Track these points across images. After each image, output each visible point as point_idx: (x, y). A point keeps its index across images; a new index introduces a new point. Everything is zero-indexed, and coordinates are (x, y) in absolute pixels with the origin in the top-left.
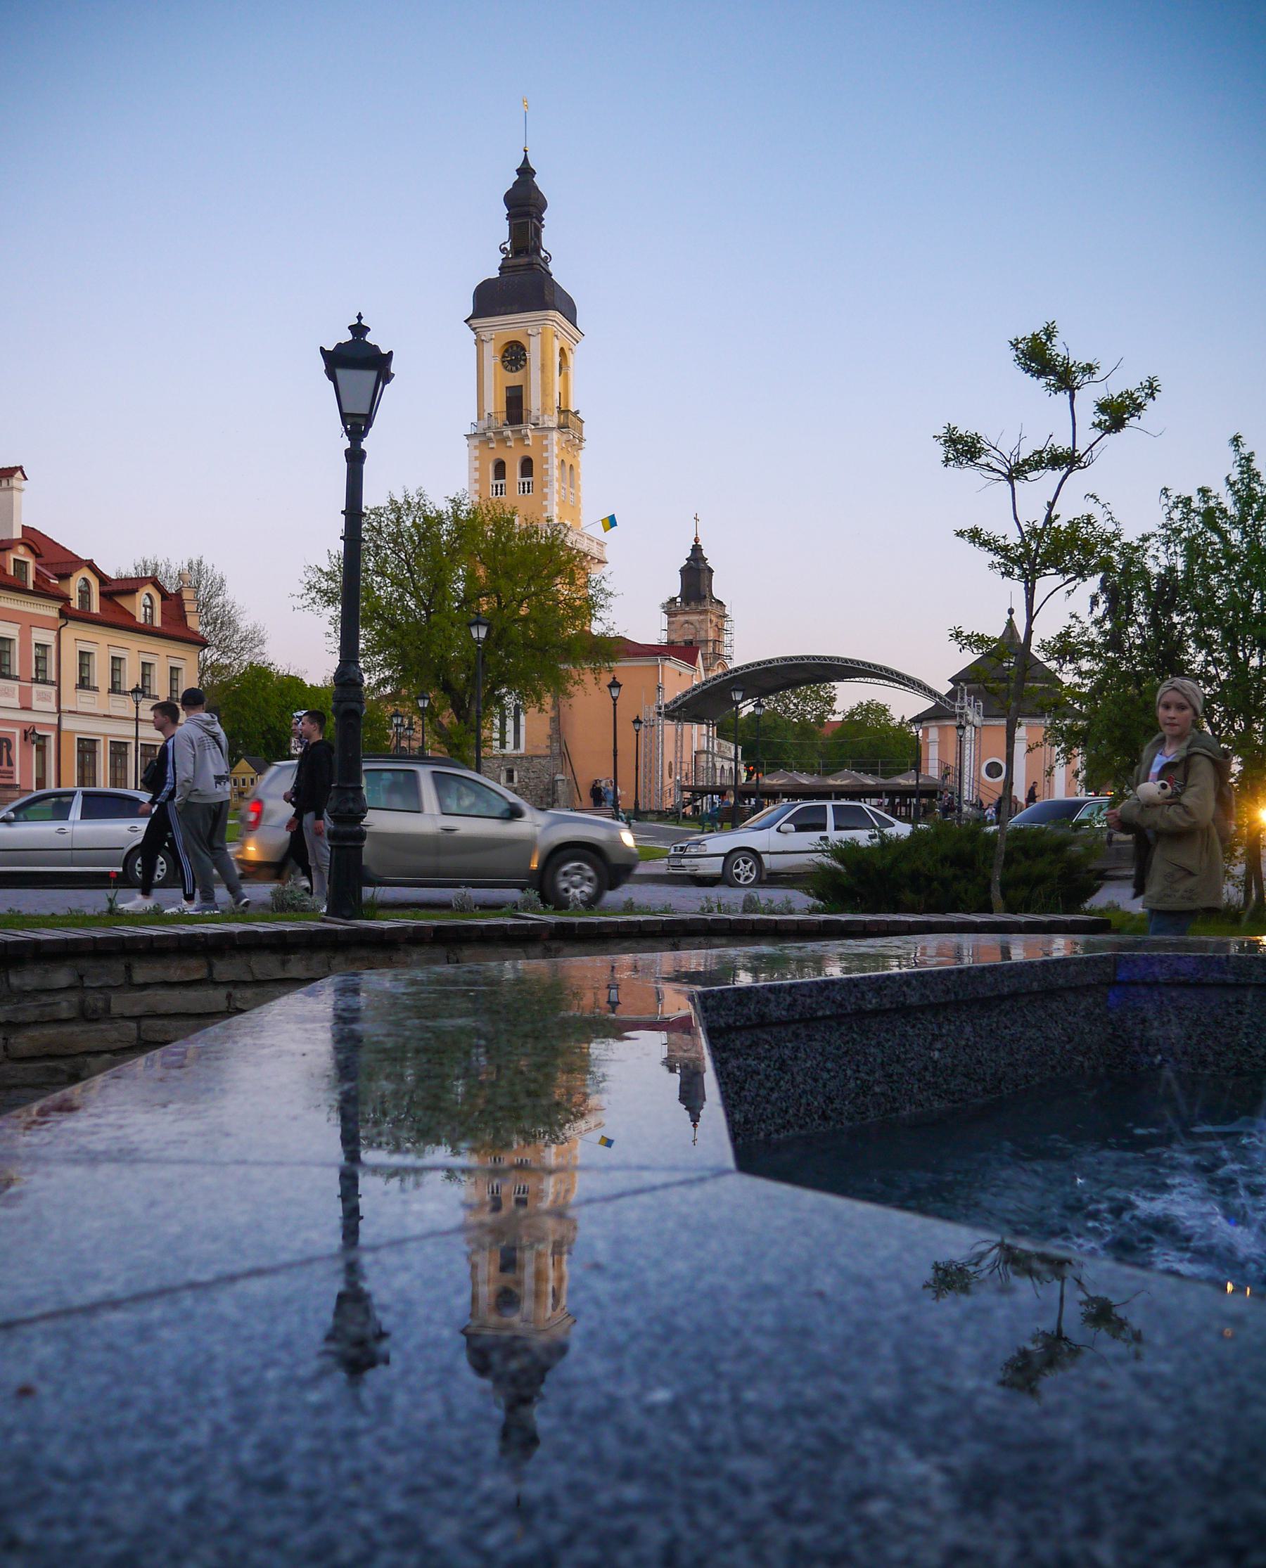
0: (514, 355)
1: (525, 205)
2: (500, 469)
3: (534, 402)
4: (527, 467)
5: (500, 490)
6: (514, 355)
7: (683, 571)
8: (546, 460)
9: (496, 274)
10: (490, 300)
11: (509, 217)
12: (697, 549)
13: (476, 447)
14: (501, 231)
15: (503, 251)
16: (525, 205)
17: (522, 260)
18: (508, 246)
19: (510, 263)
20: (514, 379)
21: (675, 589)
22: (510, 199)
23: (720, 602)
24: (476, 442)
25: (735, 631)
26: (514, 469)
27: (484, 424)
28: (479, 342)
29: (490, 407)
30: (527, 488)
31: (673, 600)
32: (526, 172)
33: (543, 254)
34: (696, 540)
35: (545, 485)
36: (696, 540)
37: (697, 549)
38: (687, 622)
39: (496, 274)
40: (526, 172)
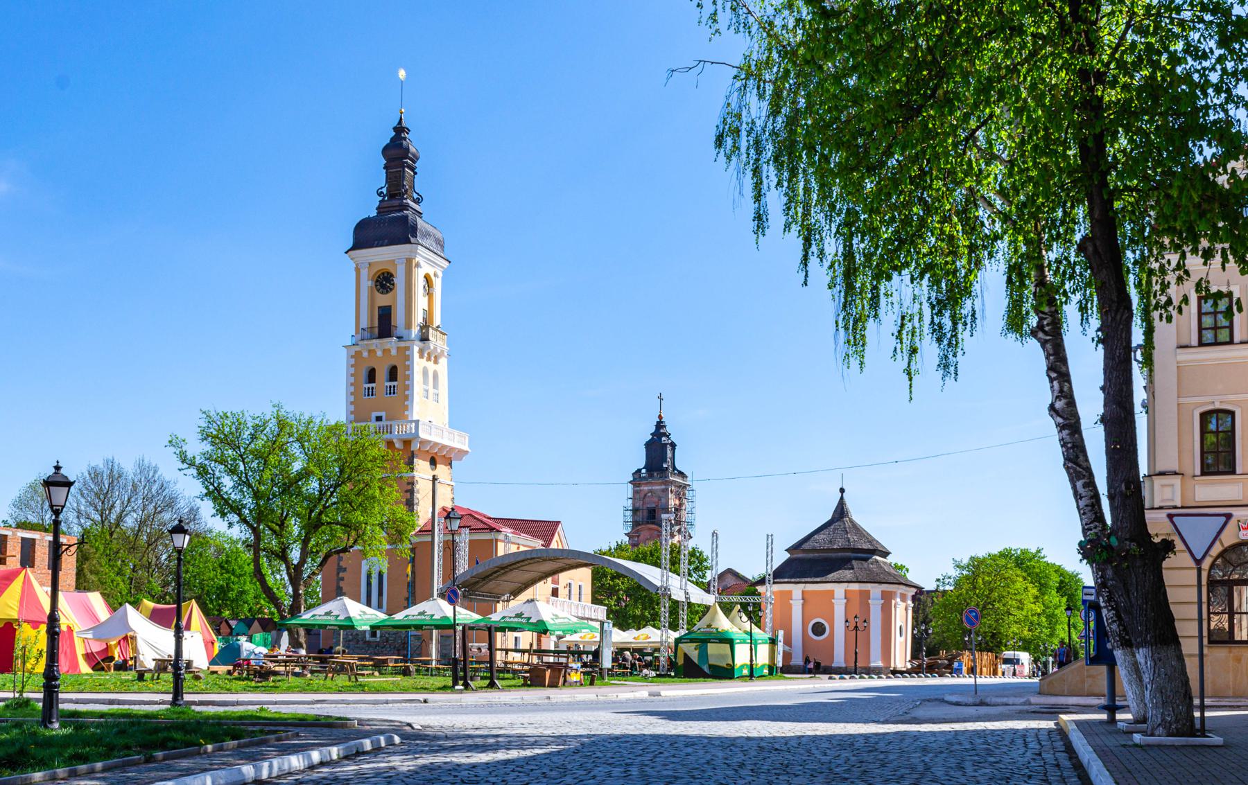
0: (384, 281)
3: (398, 318)
4: (393, 374)
5: (370, 392)
6: (384, 281)
7: (648, 445)
8: (409, 368)
9: (374, 213)
10: (367, 235)
11: (386, 167)
12: (660, 425)
14: (380, 180)
17: (396, 203)
18: (384, 190)
19: (385, 205)
20: (383, 300)
21: (639, 461)
23: (681, 474)
25: (697, 499)
26: (382, 374)
27: (359, 336)
28: (357, 270)
29: (364, 323)
30: (392, 391)
31: (639, 471)
33: (415, 196)
34: (660, 417)
35: (409, 387)
36: (660, 417)
37: (660, 425)
38: (650, 491)
39: (374, 213)
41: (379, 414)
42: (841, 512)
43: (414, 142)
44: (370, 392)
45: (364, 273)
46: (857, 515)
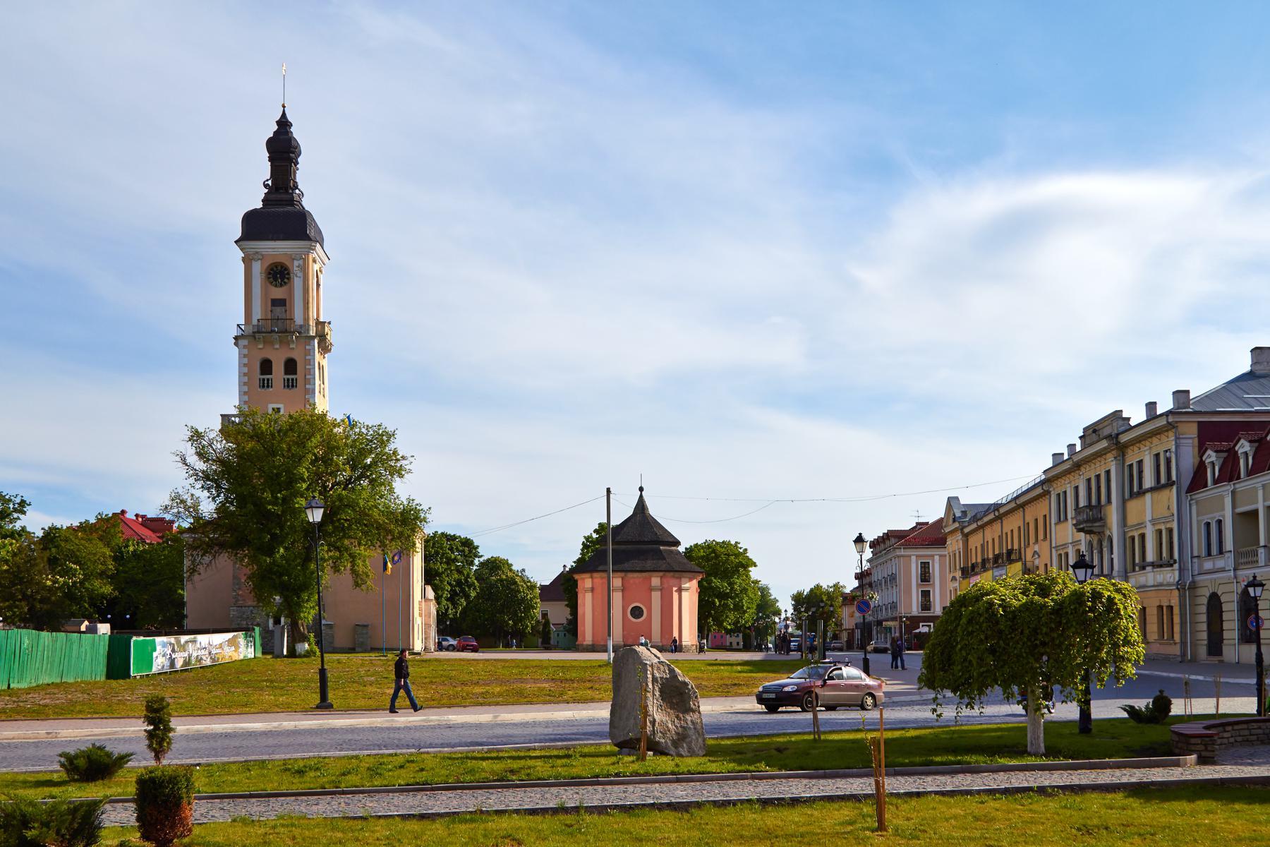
0: (279, 274)
1: (283, 149)
2: (266, 366)
4: (291, 366)
6: (279, 274)
9: (259, 205)
10: (256, 227)
11: (271, 159)
13: (245, 347)
14: (263, 169)
15: (266, 186)
16: (283, 149)
19: (273, 197)
20: (278, 293)
22: (272, 145)
24: (244, 342)
30: (290, 385)
32: (284, 124)
39: (259, 205)
40: (284, 124)
41: (275, 406)
42: (641, 506)
43: (296, 132)
44: (265, 384)
45: (257, 267)
46: (654, 511)
